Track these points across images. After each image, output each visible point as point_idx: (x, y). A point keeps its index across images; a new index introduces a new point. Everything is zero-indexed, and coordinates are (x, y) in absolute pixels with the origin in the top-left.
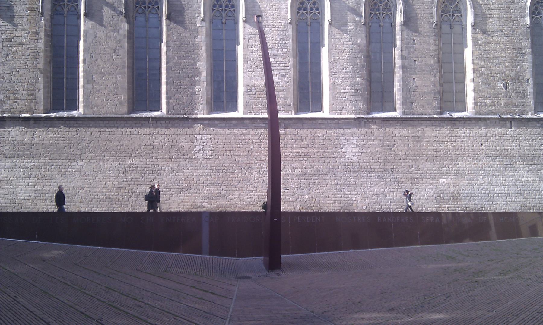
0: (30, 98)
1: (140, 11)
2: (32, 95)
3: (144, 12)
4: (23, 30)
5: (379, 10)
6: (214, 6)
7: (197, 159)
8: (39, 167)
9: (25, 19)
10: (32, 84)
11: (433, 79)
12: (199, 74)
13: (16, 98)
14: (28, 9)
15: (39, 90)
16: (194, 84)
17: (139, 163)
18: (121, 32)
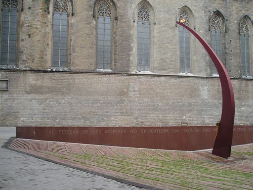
0: (41, 60)
1: (101, 14)
2: (42, 58)
3: (103, 15)
4: (38, 21)
5: (215, 24)
6: (139, 14)
7: (131, 97)
8: (46, 100)
9: (40, 14)
10: (42, 52)
11: (238, 60)
12: (132, 50)
13: (33, 59)
14: (41, 9)
15: (46, 55)
16: (129, 55)
17: (101, 98)
18: (92, 25)
